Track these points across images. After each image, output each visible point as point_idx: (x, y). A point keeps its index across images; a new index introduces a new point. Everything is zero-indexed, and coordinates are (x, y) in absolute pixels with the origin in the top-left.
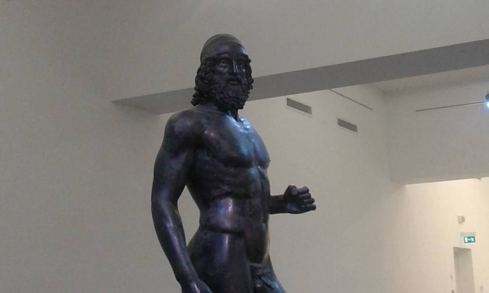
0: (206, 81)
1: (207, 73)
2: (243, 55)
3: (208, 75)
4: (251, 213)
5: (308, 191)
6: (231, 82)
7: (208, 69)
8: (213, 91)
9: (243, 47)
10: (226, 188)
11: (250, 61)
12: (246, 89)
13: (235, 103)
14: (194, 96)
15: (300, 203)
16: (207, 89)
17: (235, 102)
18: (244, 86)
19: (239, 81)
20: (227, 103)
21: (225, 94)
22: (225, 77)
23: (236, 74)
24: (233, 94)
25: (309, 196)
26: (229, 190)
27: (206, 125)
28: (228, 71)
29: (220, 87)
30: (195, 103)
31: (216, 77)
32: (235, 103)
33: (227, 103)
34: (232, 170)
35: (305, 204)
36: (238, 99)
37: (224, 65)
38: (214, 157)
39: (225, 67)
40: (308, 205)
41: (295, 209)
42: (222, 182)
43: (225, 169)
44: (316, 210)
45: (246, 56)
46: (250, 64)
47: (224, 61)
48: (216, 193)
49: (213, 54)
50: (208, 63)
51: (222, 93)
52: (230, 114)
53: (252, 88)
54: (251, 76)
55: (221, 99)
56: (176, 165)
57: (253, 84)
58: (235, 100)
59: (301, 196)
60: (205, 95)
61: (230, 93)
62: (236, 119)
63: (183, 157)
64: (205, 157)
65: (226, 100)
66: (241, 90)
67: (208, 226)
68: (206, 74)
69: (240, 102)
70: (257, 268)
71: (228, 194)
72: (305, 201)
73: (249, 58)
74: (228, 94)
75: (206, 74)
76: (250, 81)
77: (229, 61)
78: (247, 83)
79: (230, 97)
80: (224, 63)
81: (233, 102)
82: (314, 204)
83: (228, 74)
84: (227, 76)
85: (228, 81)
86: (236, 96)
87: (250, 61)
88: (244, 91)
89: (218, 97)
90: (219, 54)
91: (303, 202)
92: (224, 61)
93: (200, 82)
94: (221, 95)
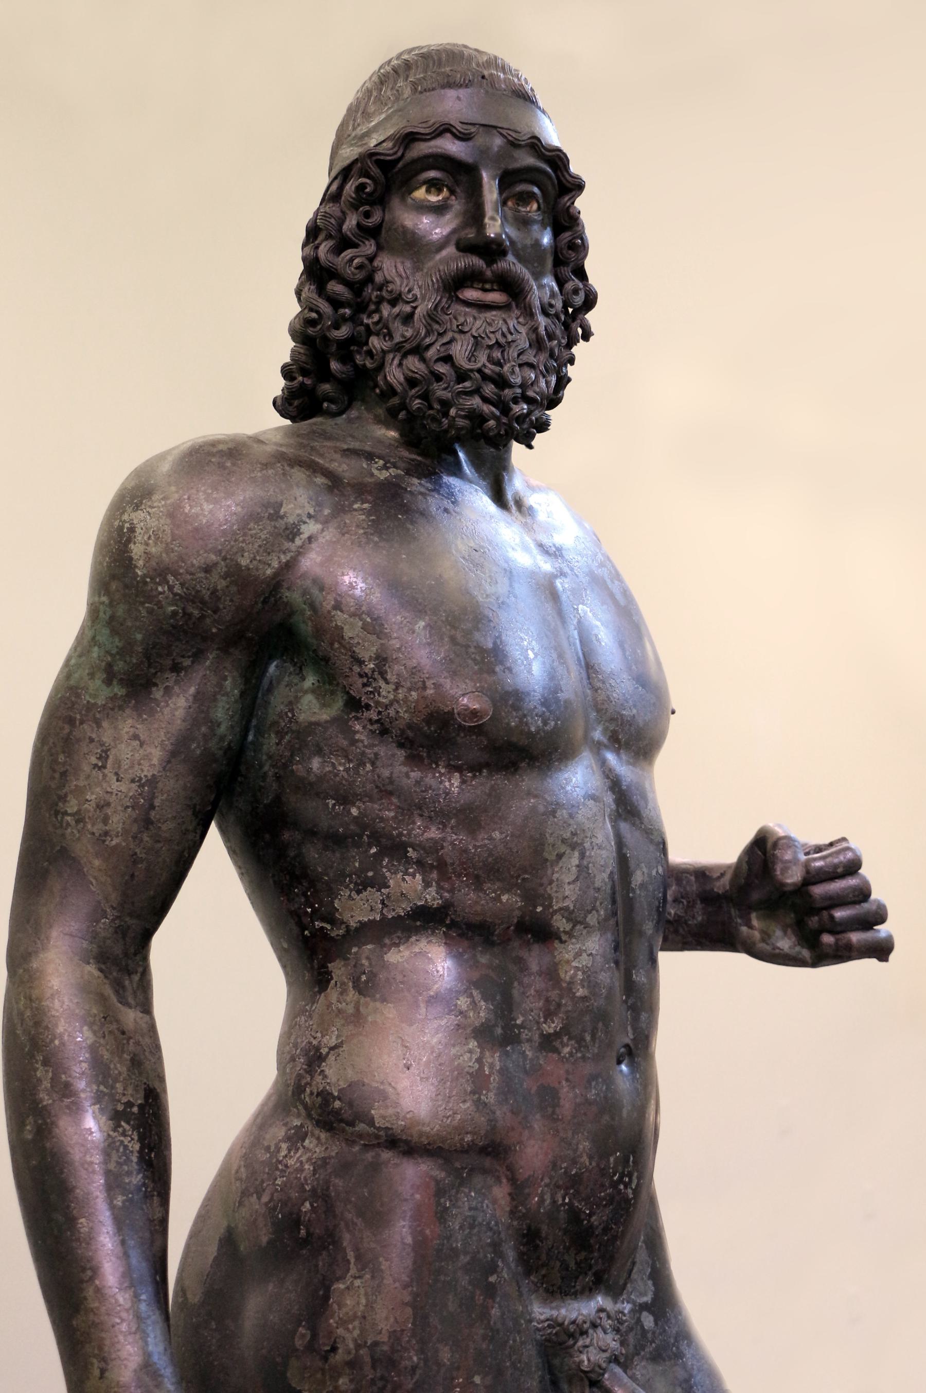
0: (335, 287)
1: (343, 244)
2: (535, 145)
3: (348, 253)
4: (550, 1028)
5: (853, 867)
6: (471, 294)
7: (351, 222)
8: (375, 343)
9: (544, 112)
10: (412, 887)
11: (578, 186)
12: (551, 336)
13: (487, 408)
14: (287, 372)
15: (813, 922)
16: (343, 332)
17: (485, 400)
18: (542, 321)
19: (514, 290)
20: (446, 405)
21: (431, 353)
22: (441, 280)
23: (491, 250)
24: (472, 357)
25: (863, 894)
26: (432, 897)
27: (310, 528)
28: (454, 231)
29: (408, 319)
30: (283, 406)
31: (391, 268)
32: (487, 408)
33: (446, 405)
34: (454, 783)
35: (837, 928)
36: (502, 382)
37: (434, 198)
38: (354, 705)
39: (439, 210)
40: (856, 937)
41: (785, 943)
42: (396, 849)
43: (415, 775)
44: (892, 957)
45: (557, 160)
46: (581, 203)
47: (432, 174)
48: (358, 908)
49: (379, 135)
50: (350, 188)
51: (419, 350)
52: (467, 469)
53: (587, 336)
54: (581, 274)
55: (412, 382)
56: (142, 748)
57: (591, 317)
58: (489, 389)
59: (818, 890)
60: (334, 365)
61: (460, 350)
62: (499, 496)
63: (176, 706)
64: (306, 702)
65: (440, 391)
66: (523, 341)
67: (315, 1097)
68: (338, 250)
69: (516, 401)
71: (425, 920)
72: (839, 914)
73: (574, 168)
74: (448, 359)
75: (338, 250)
76: (579, 300)
77: (460, 176)
78: (559, 304)
79: (462, 376)
80: (434, 185)
81: (475, 402)
82: (883, 930)
83: (451, 250)
84: (451, 260)
85: (454, 285)
86: (490, 369)
87: (578, 186)
88: (538, 344)
89: (394, 374)
90: (409, 139)
91: (832, 917)
92: (432, 174)
93: (309, 291)
94: (413, 363)
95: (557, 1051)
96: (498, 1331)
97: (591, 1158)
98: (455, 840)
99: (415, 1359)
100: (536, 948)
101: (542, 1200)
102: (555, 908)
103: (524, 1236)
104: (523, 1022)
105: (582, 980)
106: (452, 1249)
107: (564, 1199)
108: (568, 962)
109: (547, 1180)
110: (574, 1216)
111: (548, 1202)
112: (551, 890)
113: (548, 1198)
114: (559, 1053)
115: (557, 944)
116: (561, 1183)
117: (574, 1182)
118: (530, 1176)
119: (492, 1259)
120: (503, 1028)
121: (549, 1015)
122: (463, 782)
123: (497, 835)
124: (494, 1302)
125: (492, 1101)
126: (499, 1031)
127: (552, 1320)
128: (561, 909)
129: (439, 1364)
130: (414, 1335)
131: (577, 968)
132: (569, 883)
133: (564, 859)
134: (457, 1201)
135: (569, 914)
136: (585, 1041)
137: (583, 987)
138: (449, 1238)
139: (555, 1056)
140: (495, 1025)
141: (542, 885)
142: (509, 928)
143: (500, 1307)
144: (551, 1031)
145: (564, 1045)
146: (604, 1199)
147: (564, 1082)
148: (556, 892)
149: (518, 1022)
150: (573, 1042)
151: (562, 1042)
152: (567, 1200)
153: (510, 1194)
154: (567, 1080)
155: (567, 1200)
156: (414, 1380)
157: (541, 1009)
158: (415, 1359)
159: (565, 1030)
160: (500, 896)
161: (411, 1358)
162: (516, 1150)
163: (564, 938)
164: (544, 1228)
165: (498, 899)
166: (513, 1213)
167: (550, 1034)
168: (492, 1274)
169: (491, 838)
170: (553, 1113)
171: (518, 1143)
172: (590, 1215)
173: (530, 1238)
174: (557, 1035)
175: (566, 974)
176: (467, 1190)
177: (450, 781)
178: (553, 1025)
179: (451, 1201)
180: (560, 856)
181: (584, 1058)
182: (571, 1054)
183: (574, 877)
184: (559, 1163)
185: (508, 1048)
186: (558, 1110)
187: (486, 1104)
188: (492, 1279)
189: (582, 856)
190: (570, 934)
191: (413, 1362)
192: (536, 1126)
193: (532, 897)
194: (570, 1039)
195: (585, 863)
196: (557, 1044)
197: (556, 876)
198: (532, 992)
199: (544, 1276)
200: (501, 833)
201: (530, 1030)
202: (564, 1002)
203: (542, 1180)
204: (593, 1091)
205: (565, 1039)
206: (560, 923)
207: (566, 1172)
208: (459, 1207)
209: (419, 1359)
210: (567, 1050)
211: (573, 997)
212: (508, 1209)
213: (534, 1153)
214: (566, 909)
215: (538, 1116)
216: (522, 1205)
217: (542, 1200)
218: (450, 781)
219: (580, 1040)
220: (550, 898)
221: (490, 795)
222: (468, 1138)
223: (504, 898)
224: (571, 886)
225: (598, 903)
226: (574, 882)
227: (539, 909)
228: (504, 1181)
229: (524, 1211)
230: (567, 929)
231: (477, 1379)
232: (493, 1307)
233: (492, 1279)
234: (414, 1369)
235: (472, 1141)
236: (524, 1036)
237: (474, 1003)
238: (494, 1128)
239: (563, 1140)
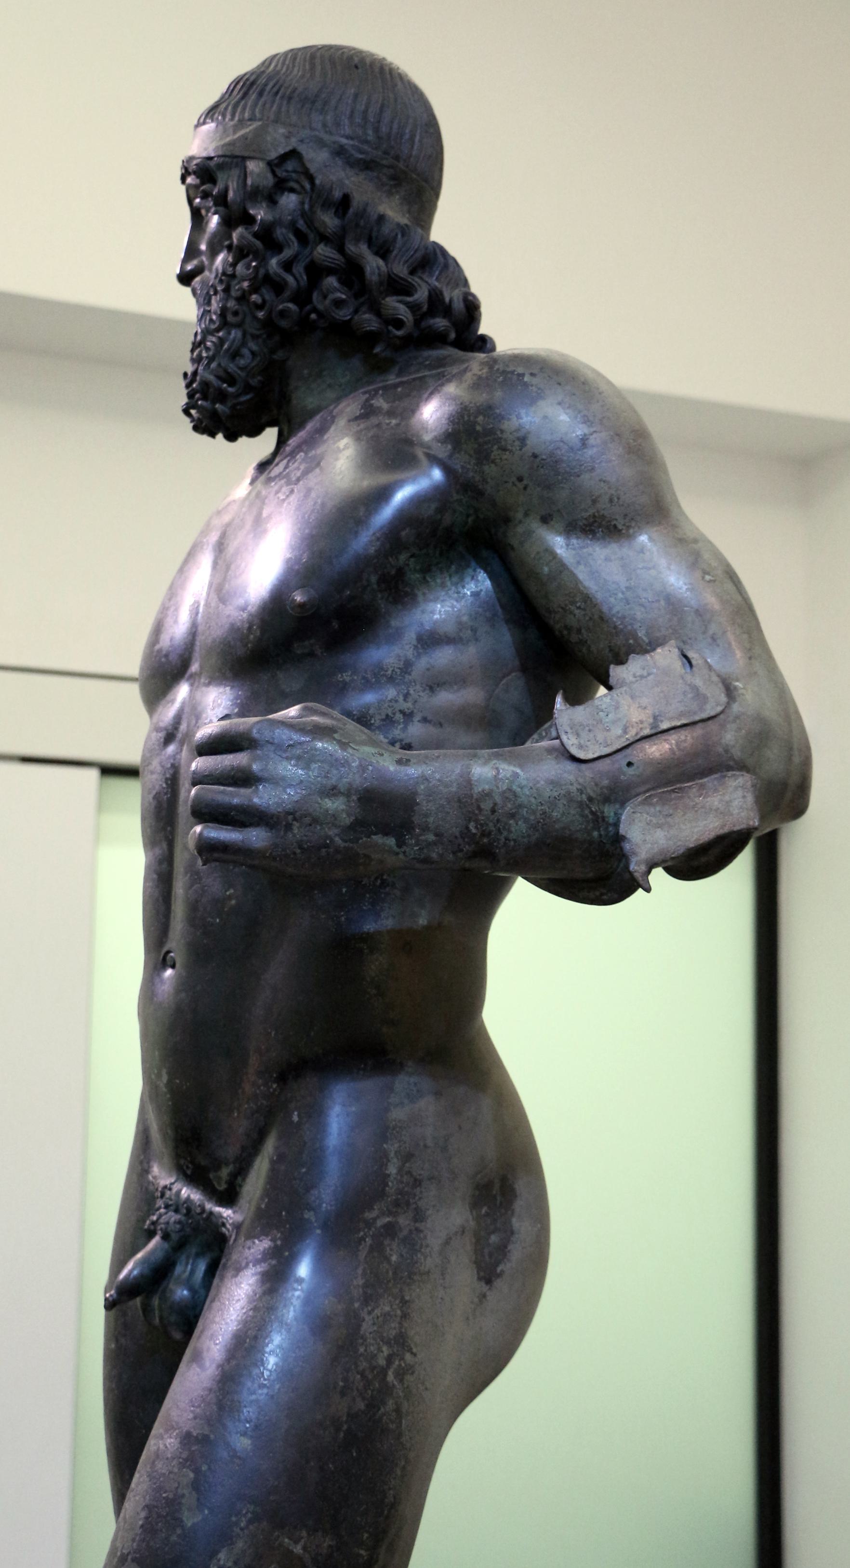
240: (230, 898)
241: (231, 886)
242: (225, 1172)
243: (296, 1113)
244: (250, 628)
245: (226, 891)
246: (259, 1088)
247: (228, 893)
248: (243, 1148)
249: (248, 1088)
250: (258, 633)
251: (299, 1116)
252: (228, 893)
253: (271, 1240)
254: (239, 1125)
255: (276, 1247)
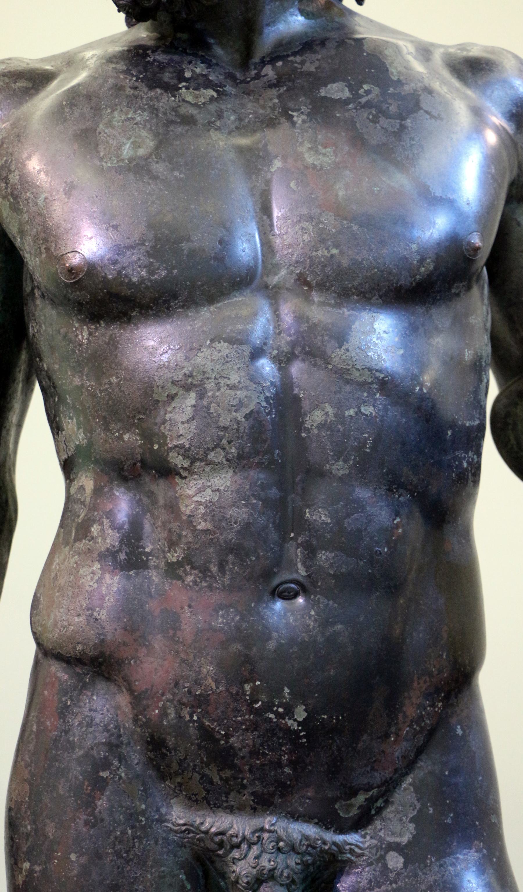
4: (174, 557)
70: (225, 843)
95: (180, 578)
96: (102, 820)
97: (217, 682)
98: (89, 386)
99: (29, 827)
100: (162, 482)
101: (164, 714)
102: (170, 446)
103: (148, 743)
104: (152, 550)
105: (204, 515)
106: (68, 741)
107: (191, 716)
108: (189, 497)
109: (169, 696)
110: (207, 734)
111: (173, 715)
112: (165, 429)
113: (172, 713)
114: (183, 581)
115: (178, 480)
116: (185, 700)
117: (201, 702)
118: (147, 690)
119: (106, 758)
120: (127, 554)
121: (172, 544)
122: (90, 334)
123: (114, 380)
124: (102, 794)
125: (103, 617)
126: (122, 556)
127: (192, 826)
128: (176, 446)
129: (46, 837)
130: (29, 807)
131: (199, 503)
132: (183, 423)
133: (176, 400)
134: (78, 701)
135: (184, 451)
136: (211, 571)
137: (205, 521)
138: (67, 732)
139: (179, 583)
140: (120, 550)
141: (156, 424)
142: (135, 464)
143: (109, 800)
144: (175, 560)
145: (187, 574)
146: (242, 723)
147: (186, 608)
148: (169, 430)
149: (147, 550)
150: (196, 572)
151: (185, 571)
152: (195, 718)
153: (131, 703)
154: (190, 606)
155: (195, 718)
156: (27, 846)
157: (165, 540)
158: (29, 827)
159: (188, 560)
160: (121, 435)
161: (26, 827)
162: (130, 663)
163: (184, 474)
164: (171, 741)
165: (120, 438)
166: (136, 720)
167: (173, 563)
168: (104, 770)
169: (110, 384)
170: (175, 635)
171: (132, 658)
172: (227, 736)
173: (156, 745)
174: (179, 564)
175: (186, 508)
176: (90, 694)
177: (82, 334)
178: (176, 555)
179: (72, 701)
180: (172, 397)
181: (210, 587)
182: (195, 582)
183: (188, 417)
184: (181, 682)
185: (131, 573)
186: (179, 633)
187: (97, 620)
188: (104, 774)
189: (201, 396)
190: (189, 470)
191: (27, 830)
192: (156, 646)
193: (148, 436)
194: (193, 568)
195: (205, 402)
196: (180, 572)
197: (168, 416)
198: (160, 524)
199: (180, 784)
200: (117, 378)
201: (157, 558)
202: (184, 533)
203: (163, 694)
204: (220, 620)
205: (188, 568)
206: (178, 460)
207: (189, 692)
208: (80, 707)
209: (32, 828)
210: (190, 578)
211: (194, 529)
212: (131, 716)
213: (153, 667)
214: (182, 446)
215: (159, 637)
216: (141, 714)
217: (164, 714)
218: (82, 334)
219: (205, 571)
220: (164, 437)
221: (108, 344)
222: (79, 647)
223: (126, 437)
224: (186, 425)
225: (224, 441)
226: (188, 421)
227: (156, 447)
228: (124, 690)
229: (144, 720)
230: (186, 465)
231: (73, 857)
232: (100, 799)
233: (104, 774)
234: (28, 835)
235: (83, 650)
236: (151, 563)
237: (103, 531)
238: (103, 641)
239: (183, 661)
240: (397, 526)
241: (397, 514)
242: (361, 799)
243: (459, 727)
244: (422, 261)
245: (394, 519)
246: (425, 708)
247: (395, 522)
248: (396, 770)
249: (410, 710)
250: (431, 267)
251: (462, 729)
252: (395, 522)
253: (477, 852)
254: (398, 749)
255: (484, 855)
